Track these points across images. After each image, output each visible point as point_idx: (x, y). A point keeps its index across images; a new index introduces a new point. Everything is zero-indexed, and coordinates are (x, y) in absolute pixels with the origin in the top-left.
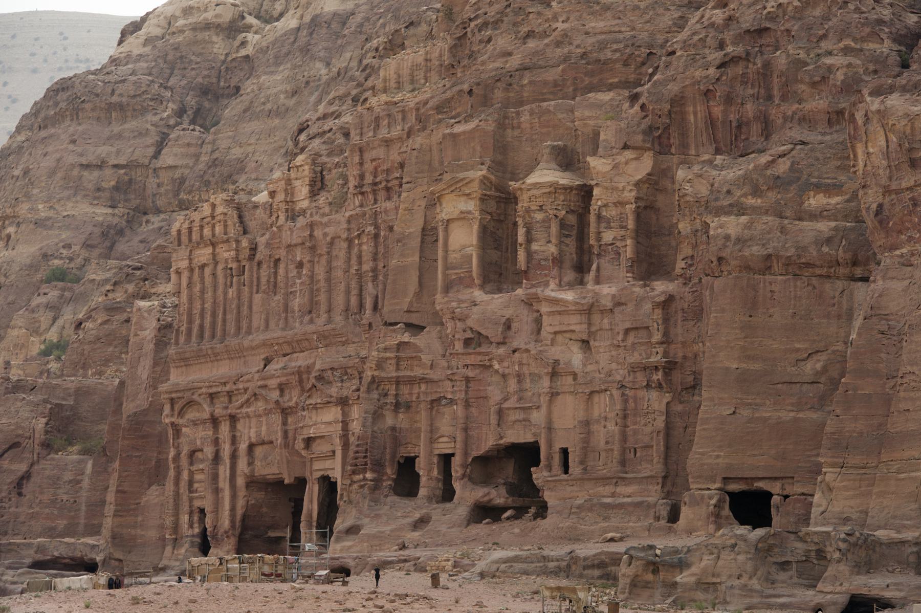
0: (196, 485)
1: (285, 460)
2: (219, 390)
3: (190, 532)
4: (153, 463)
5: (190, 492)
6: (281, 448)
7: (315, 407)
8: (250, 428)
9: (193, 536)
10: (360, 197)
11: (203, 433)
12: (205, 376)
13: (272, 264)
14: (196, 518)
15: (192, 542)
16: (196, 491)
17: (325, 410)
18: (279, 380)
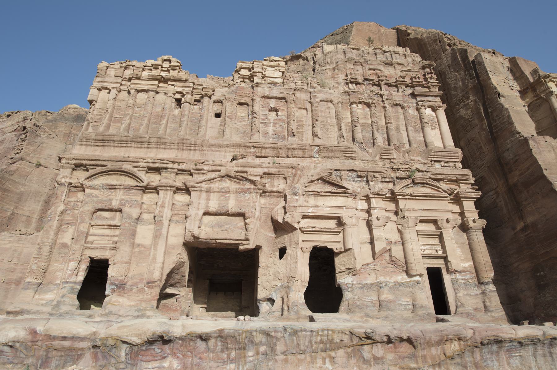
0: (90, 238)
1: (255, 230)
2: (170, 166)
3: (73, 279)
4: (9, 214)
5: (85, 242)
6: (257, 220)
7: (317, 194)
8: (208, 199)
9: (75, 283)
10: (354, 85)
11: (123, 197)
12: (142, 155)
13: (236, 105)
14: (84, 266)
15: (72, 289)
16: (92, 243)
17: (328, 198)
18: (266, 170)
